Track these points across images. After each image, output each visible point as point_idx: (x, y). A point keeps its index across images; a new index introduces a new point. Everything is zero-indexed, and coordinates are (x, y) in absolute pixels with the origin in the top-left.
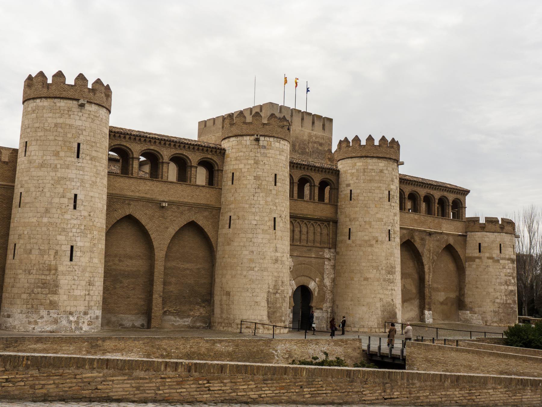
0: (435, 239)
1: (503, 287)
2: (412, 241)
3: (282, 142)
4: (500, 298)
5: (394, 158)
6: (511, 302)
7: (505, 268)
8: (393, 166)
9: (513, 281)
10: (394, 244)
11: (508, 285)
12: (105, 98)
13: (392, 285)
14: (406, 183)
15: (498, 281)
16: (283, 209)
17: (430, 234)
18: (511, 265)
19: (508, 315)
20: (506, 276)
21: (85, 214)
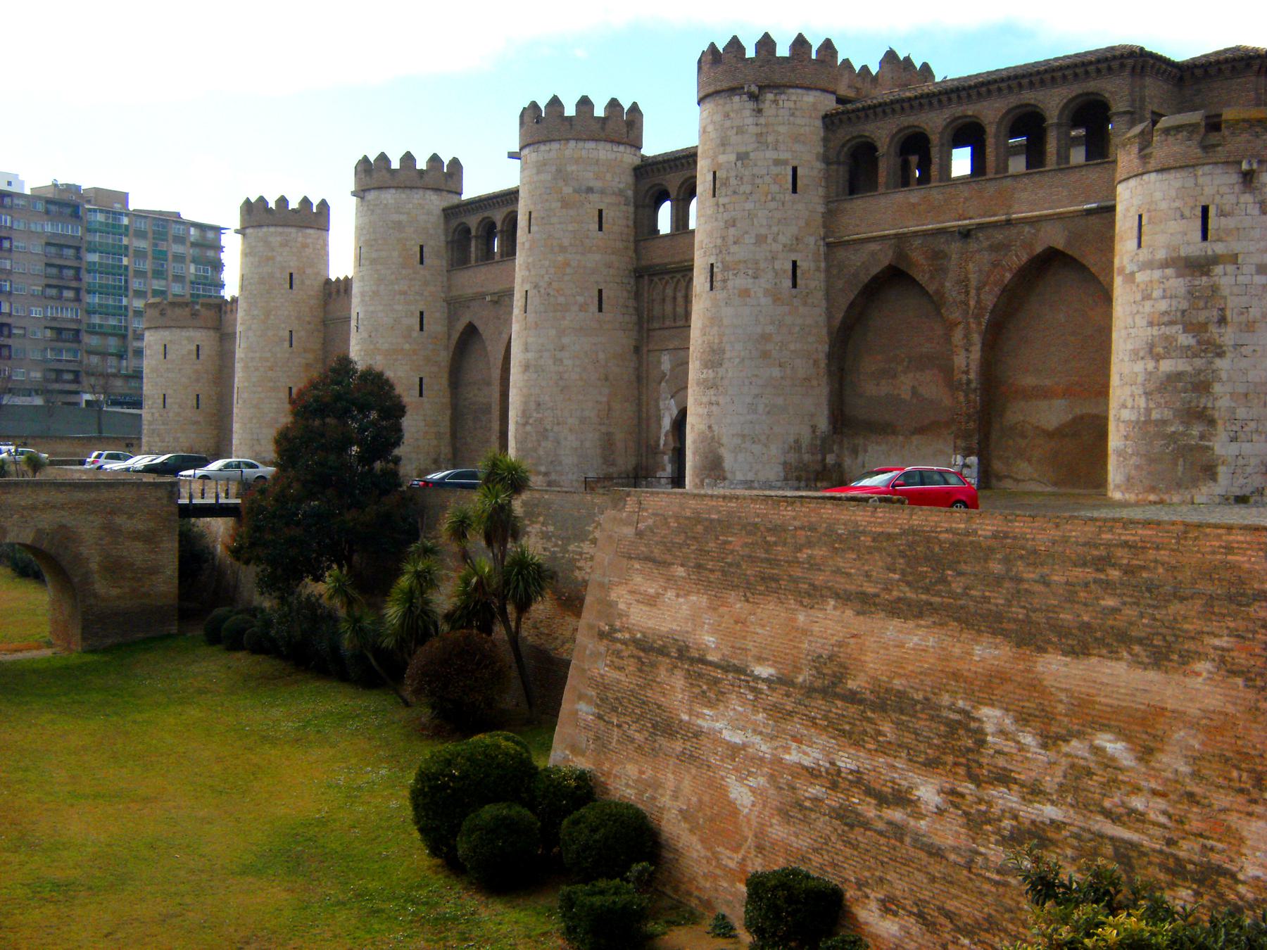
0: (986, 244)
1: (1139, 367)
2: (903, 267)
3: (543, 148)
4: (1129, 404)
5: (725, 85)
6: (1168, 414)
7: (1147, 297)
8: (728, 107)
9: (1185, 340)
10: (723, 294)
11: (1157, 358)
12: (388, 175)
13: (712, 392)
14: (875, 114)
15: (1129, 347)
16: (543, 272)
17: (966, 234)
18: (1178, 285)
19: (1151, 461)
20: (1151, 324)
21: (365, 335)
